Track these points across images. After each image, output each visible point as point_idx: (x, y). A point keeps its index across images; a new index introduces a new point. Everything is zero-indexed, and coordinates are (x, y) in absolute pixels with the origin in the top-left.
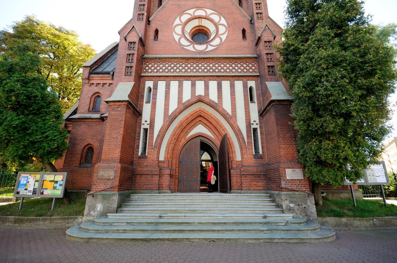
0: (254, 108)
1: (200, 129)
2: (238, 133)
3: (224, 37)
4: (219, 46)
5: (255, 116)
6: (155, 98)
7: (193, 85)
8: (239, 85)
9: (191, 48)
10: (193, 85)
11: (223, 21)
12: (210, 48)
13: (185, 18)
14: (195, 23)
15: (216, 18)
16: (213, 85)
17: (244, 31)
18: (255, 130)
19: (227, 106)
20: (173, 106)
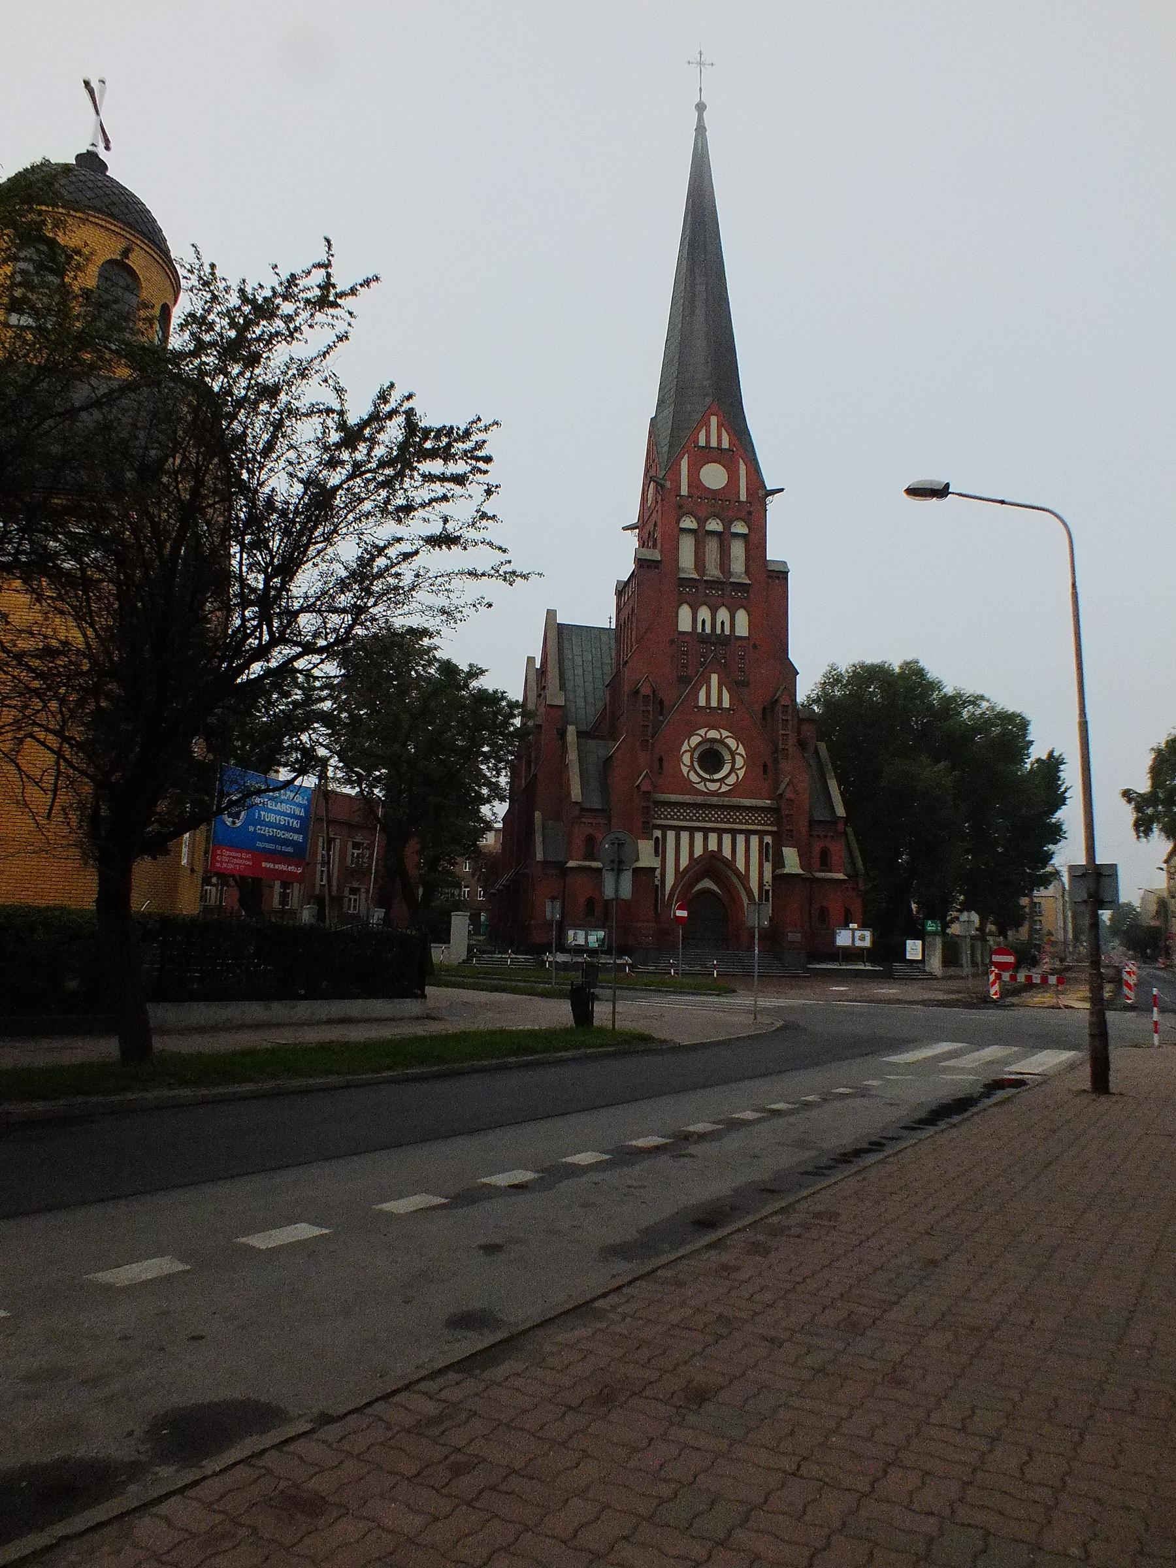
0: (768, 867)
1: (707, 884)
2: (749, 892)
3: (741, 773)
4: (736, 785)
5: (768, 876)
6: (664, 852)
7: (706, 839)
8: (754, 841)
9: (701, 787)
10: (706, 839)
11: (741, 750)
12: (724, 789)
13: (695, 740)
14: (707, 746)
15: (732, 743)
16: (727, 839)
17: (765, 766)
18: (767, 891)
19: (740, 865)
20: (684, 862)
